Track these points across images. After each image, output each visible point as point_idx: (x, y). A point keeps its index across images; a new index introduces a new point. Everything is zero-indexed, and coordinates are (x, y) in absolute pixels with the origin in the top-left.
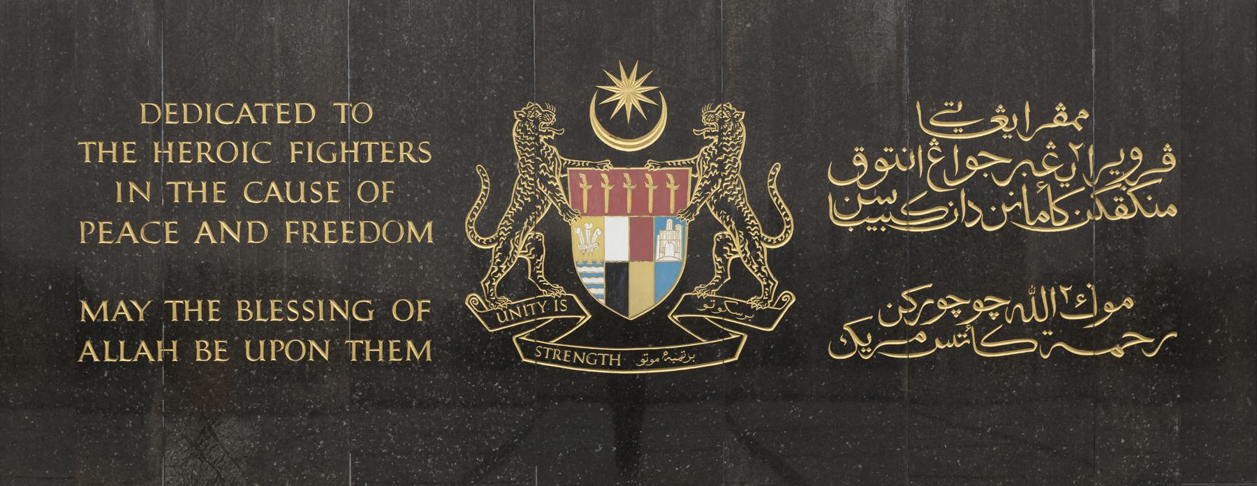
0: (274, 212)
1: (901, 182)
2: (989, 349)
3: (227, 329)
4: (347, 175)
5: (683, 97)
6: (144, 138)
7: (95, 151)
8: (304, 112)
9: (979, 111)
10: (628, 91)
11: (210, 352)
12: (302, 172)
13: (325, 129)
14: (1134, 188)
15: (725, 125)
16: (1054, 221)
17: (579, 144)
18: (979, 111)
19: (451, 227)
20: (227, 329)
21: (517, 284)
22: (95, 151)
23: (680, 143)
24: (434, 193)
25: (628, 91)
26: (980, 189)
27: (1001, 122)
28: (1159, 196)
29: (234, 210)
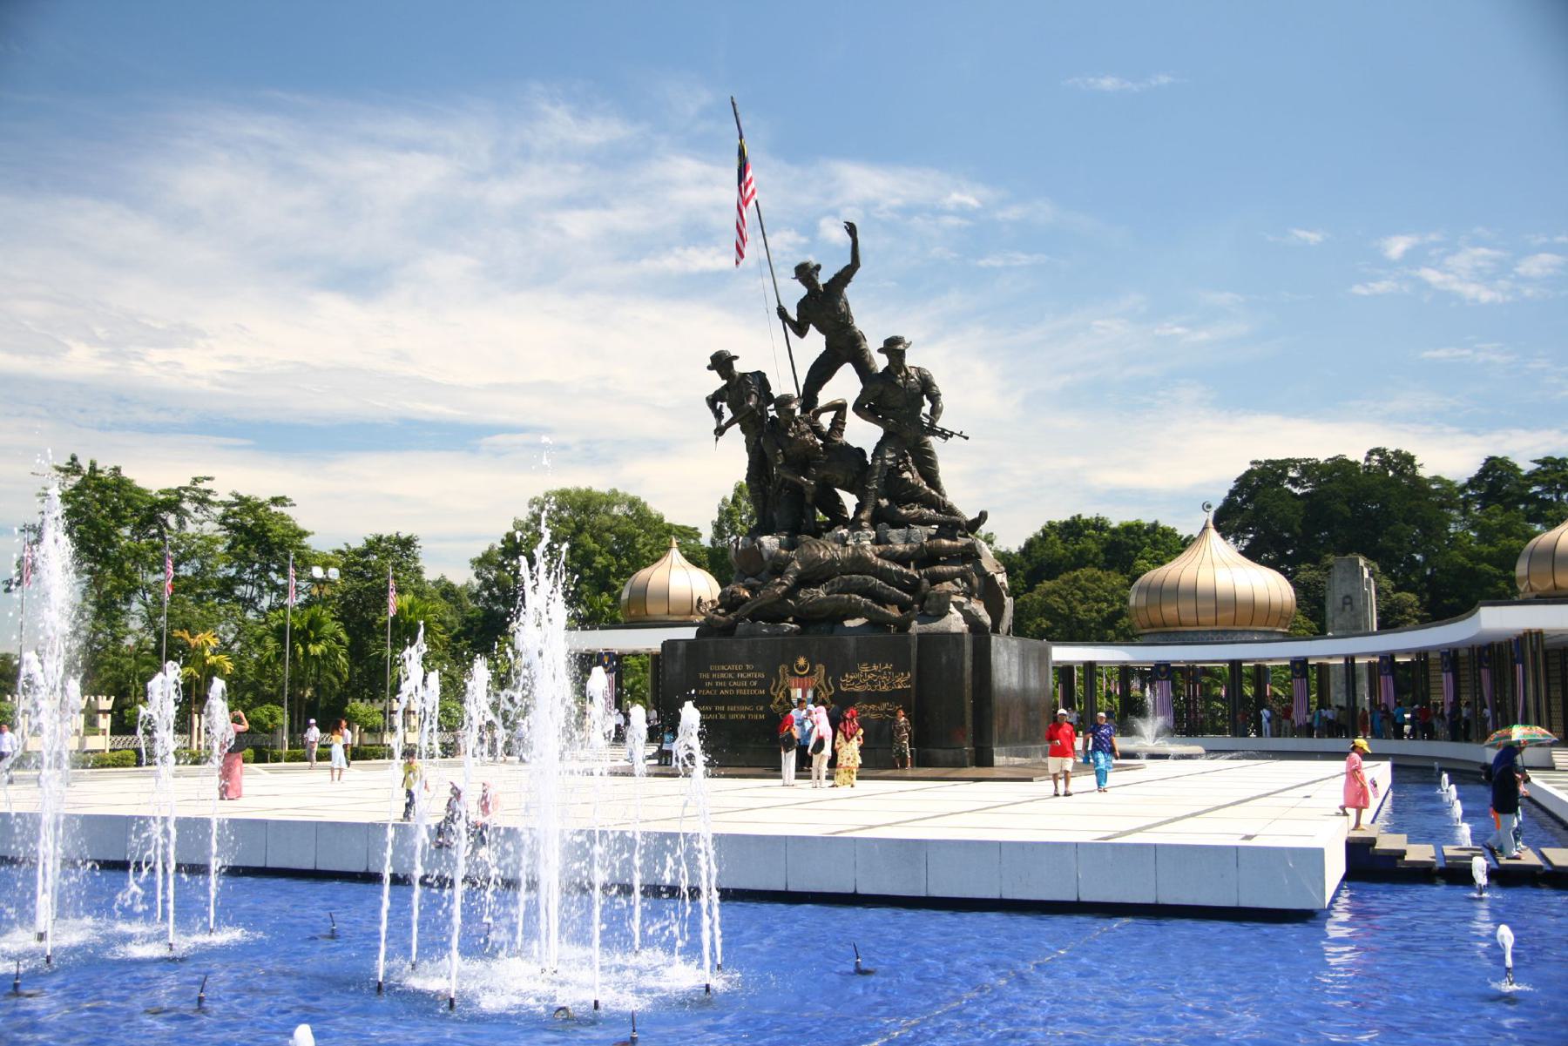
0: (735, 688)
1: (856, 681)
2: (873, 716)
3: (726, 712)
4: (749, 680)
5: (812, 662)
6: (711, 673)
7: (702, 676)
8: (740, 667)
9: (870, 665)
10: (802, 662)
11: (722, 717)
12: (740, 679)
13: (745, 671)
14: (902, 682)
15: (821, 669)
16: (885, 688)
17: (792, 674)
18: (870, 665)
19: (768, 691)
20: (726, 712)
21: (780, 703)
22: (702, 676)
23: (811, 673)
24: (763, 684)
25: (802, 662)
26: (871, 682)
27: (875, 668)
28: (907, 682)
29: (728, 688)
